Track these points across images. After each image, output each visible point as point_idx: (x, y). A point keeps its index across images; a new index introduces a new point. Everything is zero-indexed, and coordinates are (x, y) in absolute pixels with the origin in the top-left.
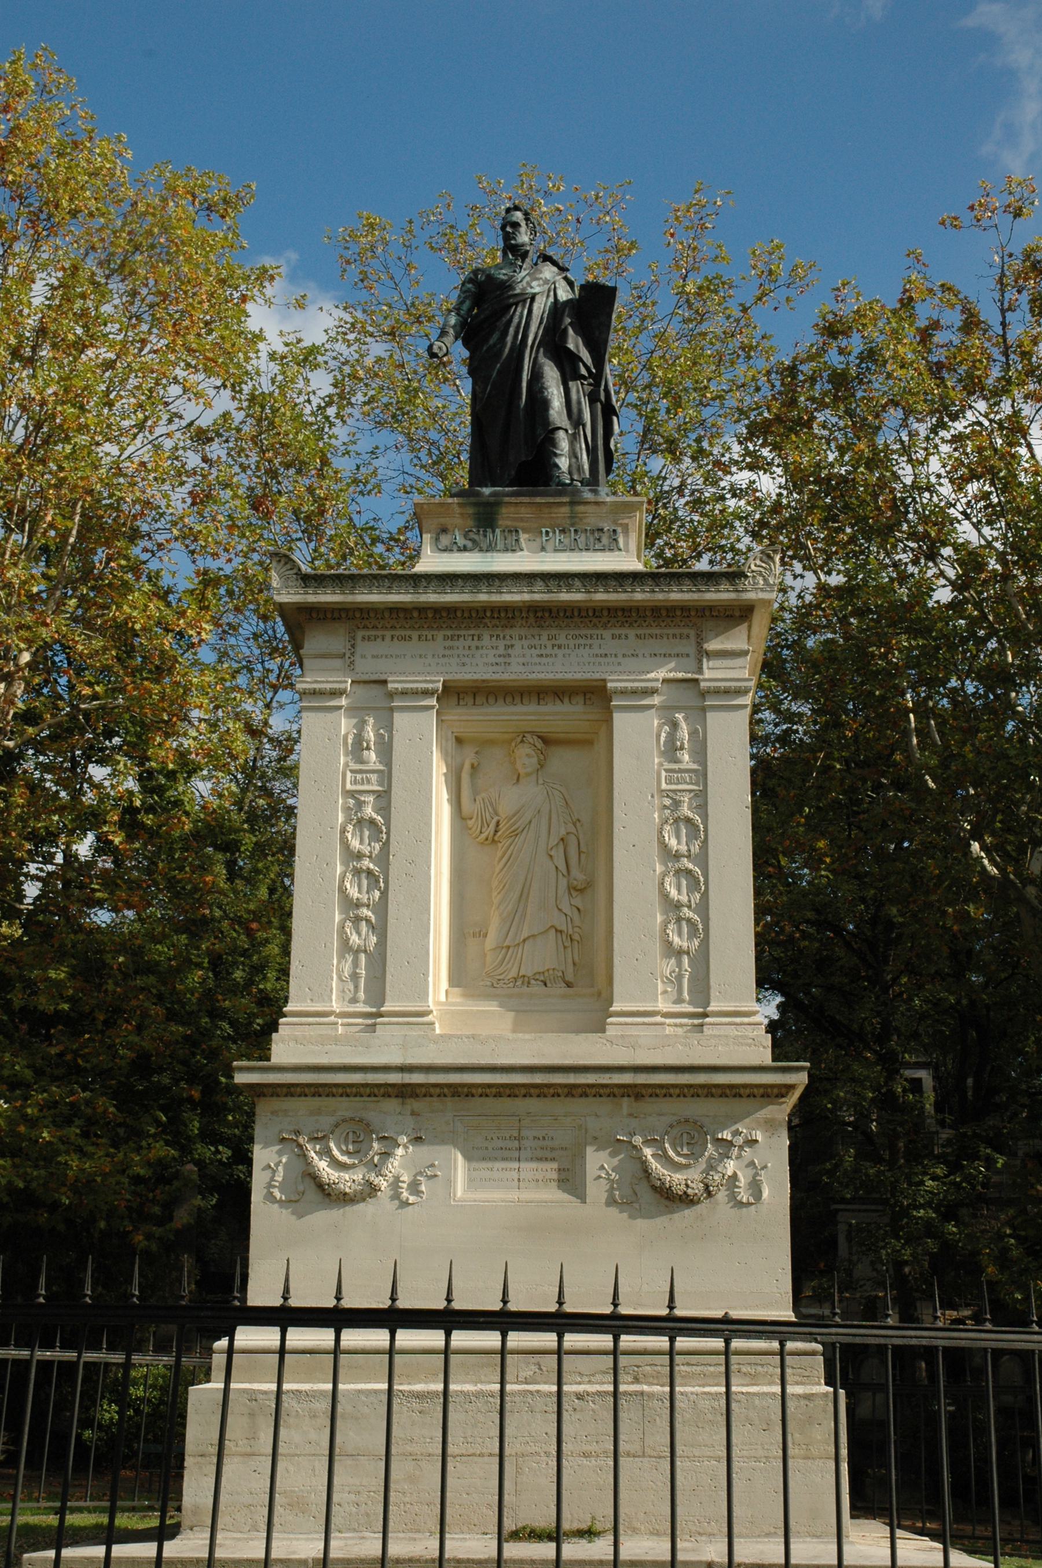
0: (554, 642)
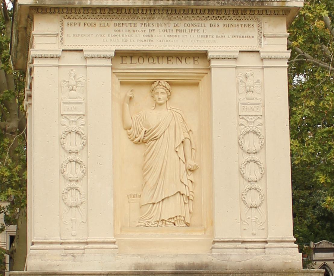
0: (177, 28)
